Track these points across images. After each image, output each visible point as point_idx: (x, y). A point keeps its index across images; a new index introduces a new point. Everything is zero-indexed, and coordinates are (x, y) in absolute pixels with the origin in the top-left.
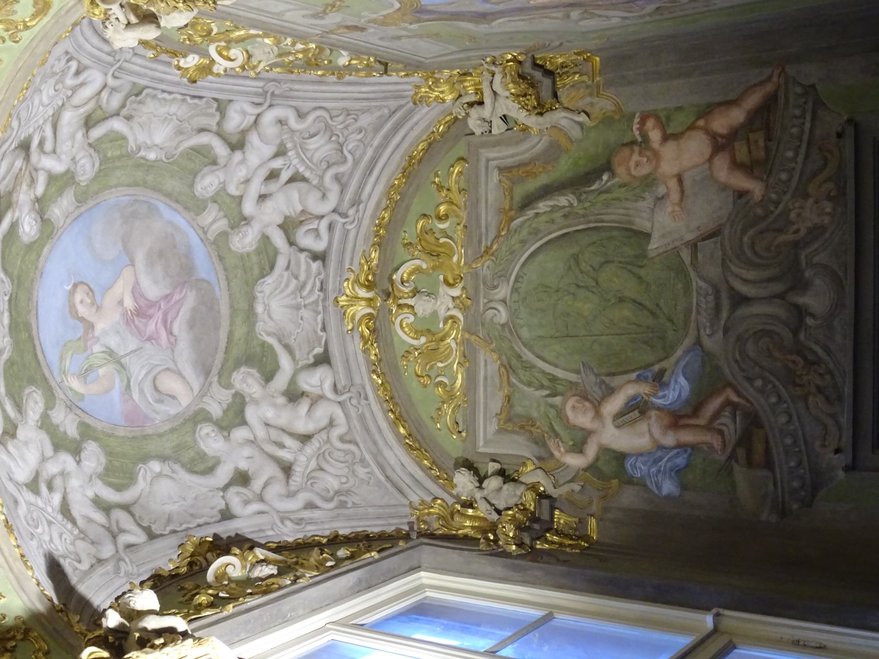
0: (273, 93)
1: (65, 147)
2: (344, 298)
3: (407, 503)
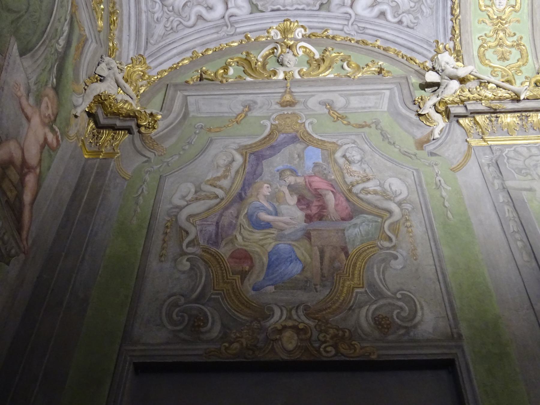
0: (227, 27)
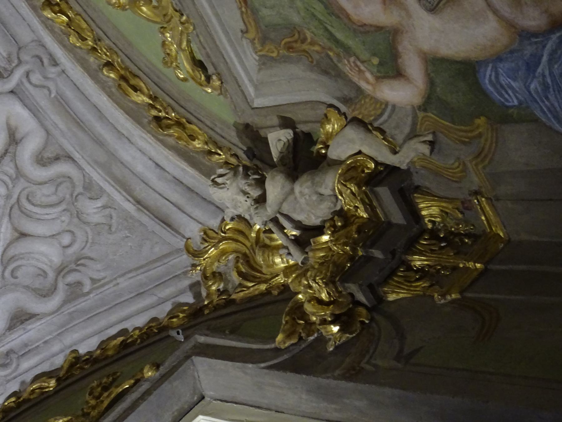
3: (181, 244)
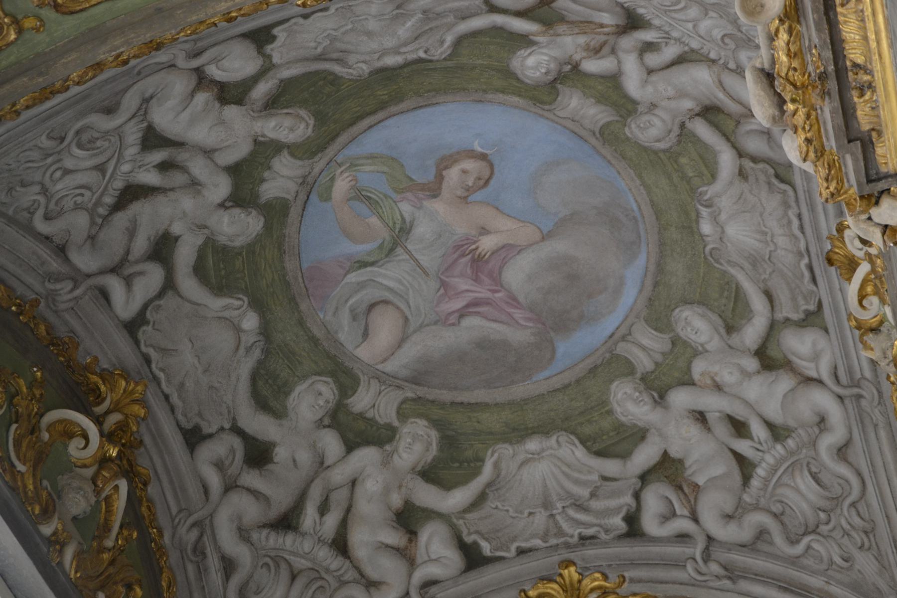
0: (859, 397)
1: (662, 86)
2: (576, 577)
